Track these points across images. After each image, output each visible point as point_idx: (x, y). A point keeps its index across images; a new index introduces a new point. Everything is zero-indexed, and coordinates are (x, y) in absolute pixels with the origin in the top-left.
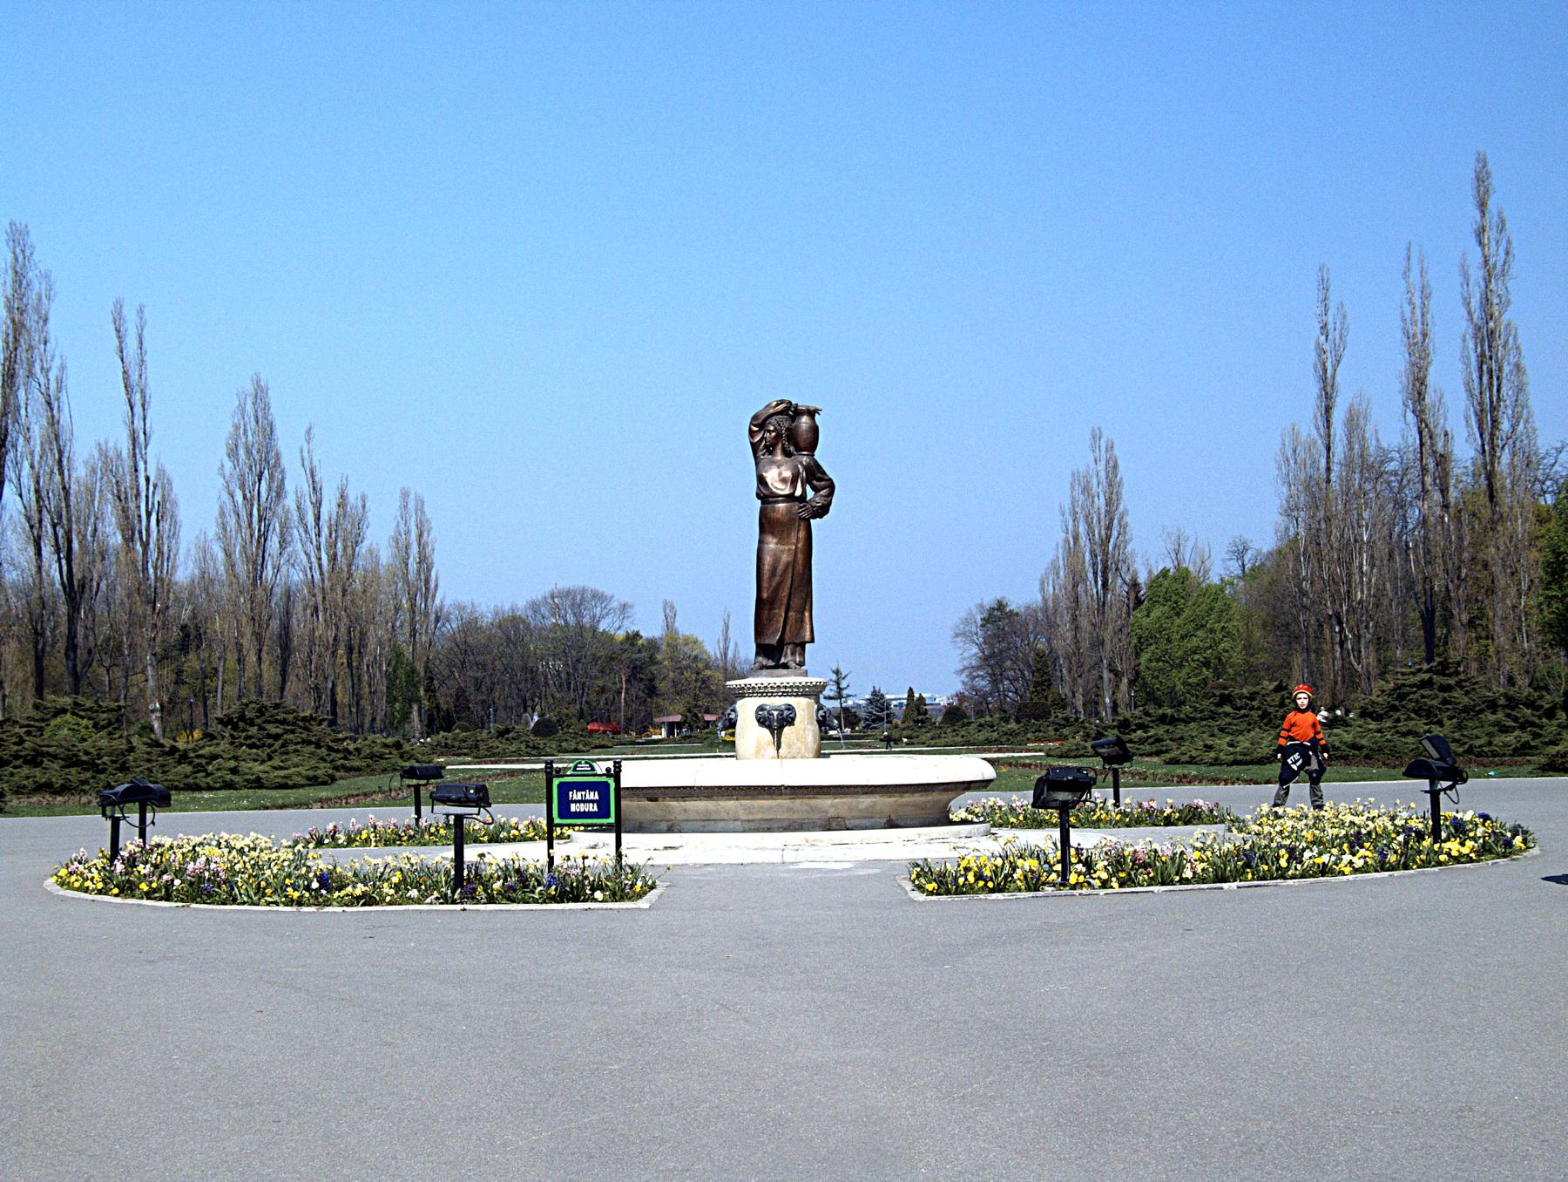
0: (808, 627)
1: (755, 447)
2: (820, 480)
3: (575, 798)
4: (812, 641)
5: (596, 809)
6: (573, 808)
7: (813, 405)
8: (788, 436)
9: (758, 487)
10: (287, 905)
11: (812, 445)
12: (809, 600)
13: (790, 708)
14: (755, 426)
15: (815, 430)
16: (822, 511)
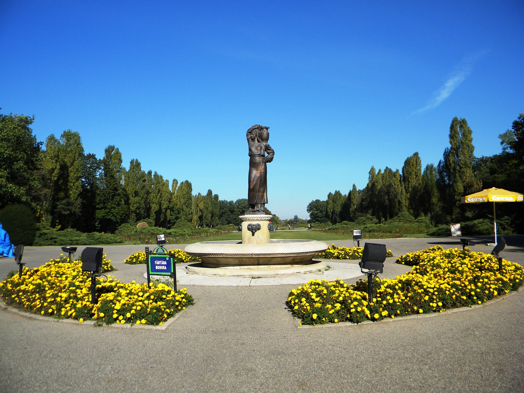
0: (266, 195)
1: (248, 139)
2: (270, 150)
3: (157, 263)
4: (267, 203)
5: (166, 268)
6: (157, 267)
7: (267, 126)
8: (259, 136)
9: (249, 153)
10: (190, 262)
11: (267, 139)
12: (266, 189)
13: (259, 225)
14: (248, 133)
15: (268, 134)
16: (270, 160)
